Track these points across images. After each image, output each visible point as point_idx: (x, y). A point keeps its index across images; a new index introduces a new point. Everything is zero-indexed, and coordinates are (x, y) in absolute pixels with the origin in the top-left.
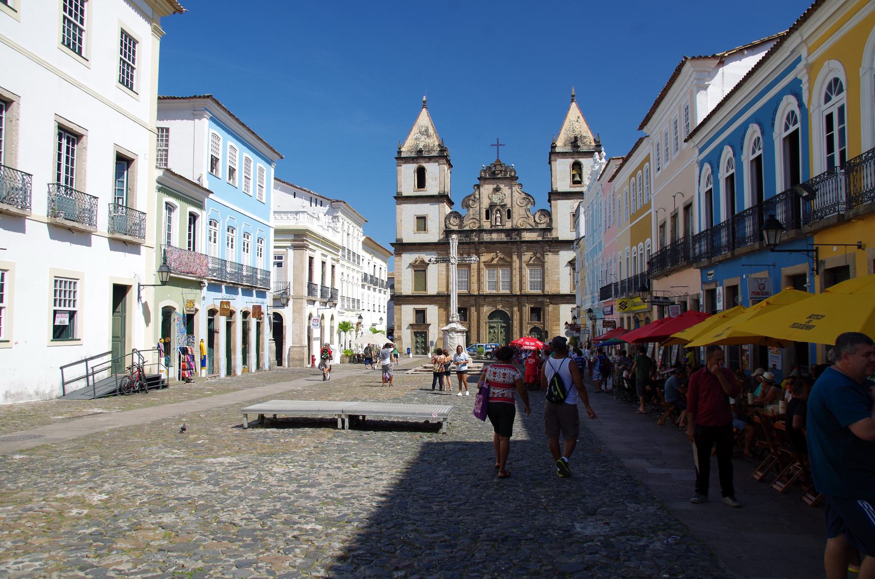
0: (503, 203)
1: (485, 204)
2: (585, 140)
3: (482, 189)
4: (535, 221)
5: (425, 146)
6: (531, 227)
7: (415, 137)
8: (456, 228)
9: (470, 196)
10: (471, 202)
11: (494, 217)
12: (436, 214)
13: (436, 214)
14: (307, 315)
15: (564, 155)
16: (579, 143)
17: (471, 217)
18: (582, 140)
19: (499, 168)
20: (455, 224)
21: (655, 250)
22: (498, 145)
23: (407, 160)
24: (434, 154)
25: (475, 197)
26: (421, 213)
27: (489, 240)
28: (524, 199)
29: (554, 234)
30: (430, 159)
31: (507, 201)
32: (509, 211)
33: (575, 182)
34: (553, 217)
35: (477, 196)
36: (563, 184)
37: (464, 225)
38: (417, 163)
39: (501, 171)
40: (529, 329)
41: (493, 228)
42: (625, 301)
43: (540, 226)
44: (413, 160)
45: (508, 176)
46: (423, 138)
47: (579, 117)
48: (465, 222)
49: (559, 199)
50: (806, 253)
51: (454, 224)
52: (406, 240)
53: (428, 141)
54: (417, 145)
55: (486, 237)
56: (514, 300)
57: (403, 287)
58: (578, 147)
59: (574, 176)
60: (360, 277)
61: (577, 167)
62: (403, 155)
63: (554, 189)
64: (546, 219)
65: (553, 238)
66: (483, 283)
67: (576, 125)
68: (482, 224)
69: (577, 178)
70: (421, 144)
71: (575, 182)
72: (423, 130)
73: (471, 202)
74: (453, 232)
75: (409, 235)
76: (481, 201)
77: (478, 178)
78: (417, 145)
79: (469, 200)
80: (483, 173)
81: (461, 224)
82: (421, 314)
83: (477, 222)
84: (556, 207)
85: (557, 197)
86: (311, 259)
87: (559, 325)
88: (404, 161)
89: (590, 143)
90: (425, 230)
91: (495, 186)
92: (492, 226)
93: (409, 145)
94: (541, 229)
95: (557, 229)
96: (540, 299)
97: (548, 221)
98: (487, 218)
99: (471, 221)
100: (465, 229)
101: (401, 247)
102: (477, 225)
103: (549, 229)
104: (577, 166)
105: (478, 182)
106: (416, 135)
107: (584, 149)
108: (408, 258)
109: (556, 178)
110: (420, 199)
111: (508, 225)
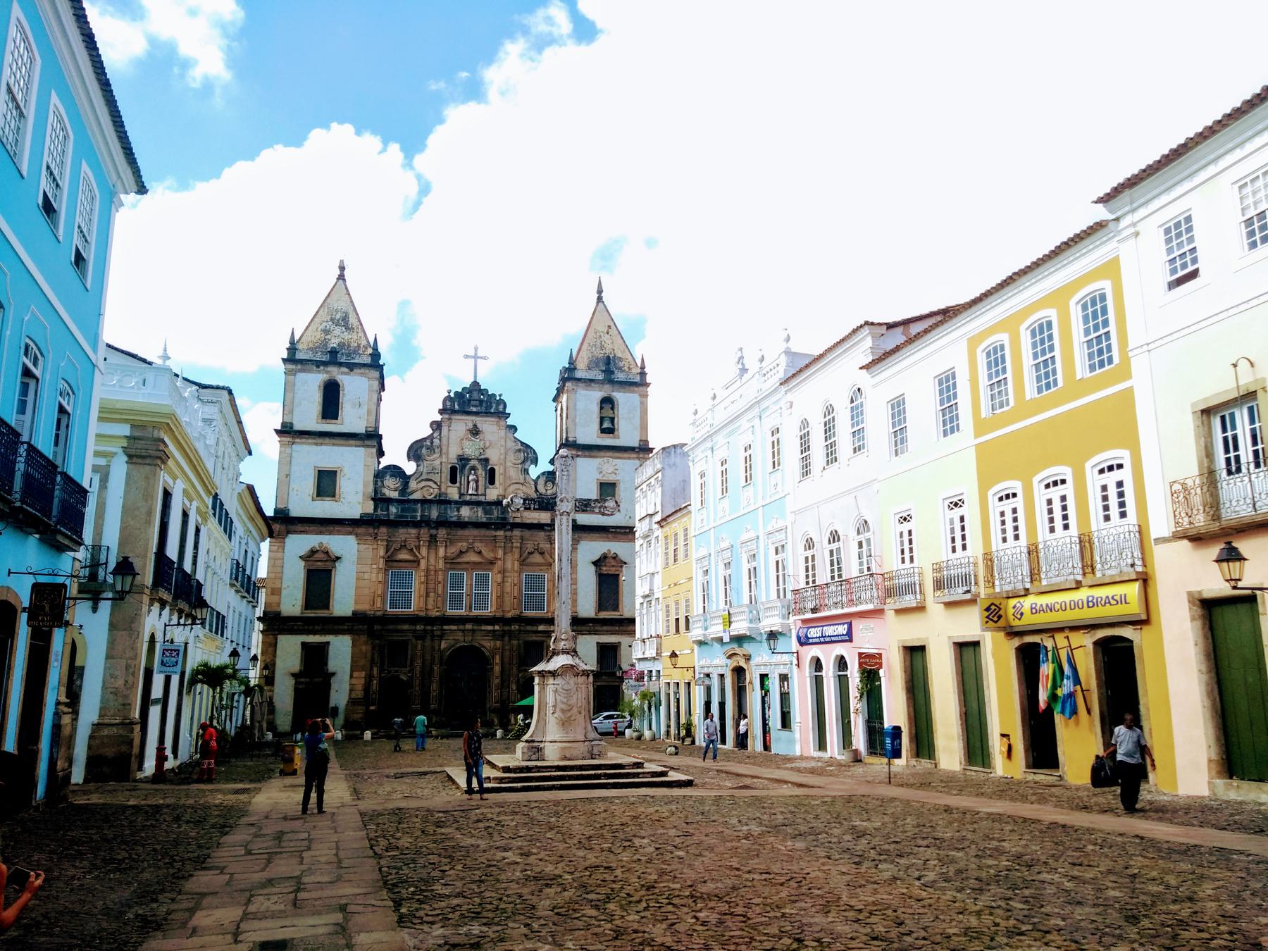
2: (621, 364)
3: (445, 430)
4: (536, 490)
5: (342, 345)
7: (323, 327)
8: (395, 495)
9: (425, 439)
10: (424, 451)
11: (464, 482)
16: (612, 367)
17: (424, 477)
18: (615, 364)
19: (475, 395)
20: (392, 486)
22: (476, 357)
25: (432, 443)
26: (327, 465)
27: (454, 519)
28: (519, 450)
30: (351, 367)
31: (494, 456)
32: (492, 471)
33: (603, 431)
35: (436, 442)
36: (589, 433)
37: (409, 490)
38: (327, 372)
39: (481, 402)
41: (468, 498)
44: (318, 367)
45: (492, 411)
46: (338, 331)
47: (609, 327)
48: (413, 485)
49: (578, 456)
51: (391, 489)
52: (295, 512)
53: (346, 336)
54: (326, 342)
55: (453, 515)
56: (497, 627)
57: (283, 600)
59: (602, 420)
62: (300, 356)
63: (571, 439)
66: (420, 596)
67: (606, 338)
69: (606, 425)
70: (333, 341)
71: (603, 431)
73: (424, 451)
74: (389, 501)
75: (305, 504)
78: (326, 342)
80: (448, 403)
81: (404, 489)
82: (315, 658)
83: (434, 486)
86: (167, 495)
88: (299, 367)
90: (334, 496)
91: (470, 426)
92: (461, 495)
93: (310, 339)
98: (453, 480)
99: (423, 484)
100: (411, 497)
102: (436, 491)
104: (607, 402)
105: (438, 418)
106: (325, 324)
107: (620, 376)
108: (299, 544)
109: (574, 420)
110: (327, 440)
111: (493, 494)
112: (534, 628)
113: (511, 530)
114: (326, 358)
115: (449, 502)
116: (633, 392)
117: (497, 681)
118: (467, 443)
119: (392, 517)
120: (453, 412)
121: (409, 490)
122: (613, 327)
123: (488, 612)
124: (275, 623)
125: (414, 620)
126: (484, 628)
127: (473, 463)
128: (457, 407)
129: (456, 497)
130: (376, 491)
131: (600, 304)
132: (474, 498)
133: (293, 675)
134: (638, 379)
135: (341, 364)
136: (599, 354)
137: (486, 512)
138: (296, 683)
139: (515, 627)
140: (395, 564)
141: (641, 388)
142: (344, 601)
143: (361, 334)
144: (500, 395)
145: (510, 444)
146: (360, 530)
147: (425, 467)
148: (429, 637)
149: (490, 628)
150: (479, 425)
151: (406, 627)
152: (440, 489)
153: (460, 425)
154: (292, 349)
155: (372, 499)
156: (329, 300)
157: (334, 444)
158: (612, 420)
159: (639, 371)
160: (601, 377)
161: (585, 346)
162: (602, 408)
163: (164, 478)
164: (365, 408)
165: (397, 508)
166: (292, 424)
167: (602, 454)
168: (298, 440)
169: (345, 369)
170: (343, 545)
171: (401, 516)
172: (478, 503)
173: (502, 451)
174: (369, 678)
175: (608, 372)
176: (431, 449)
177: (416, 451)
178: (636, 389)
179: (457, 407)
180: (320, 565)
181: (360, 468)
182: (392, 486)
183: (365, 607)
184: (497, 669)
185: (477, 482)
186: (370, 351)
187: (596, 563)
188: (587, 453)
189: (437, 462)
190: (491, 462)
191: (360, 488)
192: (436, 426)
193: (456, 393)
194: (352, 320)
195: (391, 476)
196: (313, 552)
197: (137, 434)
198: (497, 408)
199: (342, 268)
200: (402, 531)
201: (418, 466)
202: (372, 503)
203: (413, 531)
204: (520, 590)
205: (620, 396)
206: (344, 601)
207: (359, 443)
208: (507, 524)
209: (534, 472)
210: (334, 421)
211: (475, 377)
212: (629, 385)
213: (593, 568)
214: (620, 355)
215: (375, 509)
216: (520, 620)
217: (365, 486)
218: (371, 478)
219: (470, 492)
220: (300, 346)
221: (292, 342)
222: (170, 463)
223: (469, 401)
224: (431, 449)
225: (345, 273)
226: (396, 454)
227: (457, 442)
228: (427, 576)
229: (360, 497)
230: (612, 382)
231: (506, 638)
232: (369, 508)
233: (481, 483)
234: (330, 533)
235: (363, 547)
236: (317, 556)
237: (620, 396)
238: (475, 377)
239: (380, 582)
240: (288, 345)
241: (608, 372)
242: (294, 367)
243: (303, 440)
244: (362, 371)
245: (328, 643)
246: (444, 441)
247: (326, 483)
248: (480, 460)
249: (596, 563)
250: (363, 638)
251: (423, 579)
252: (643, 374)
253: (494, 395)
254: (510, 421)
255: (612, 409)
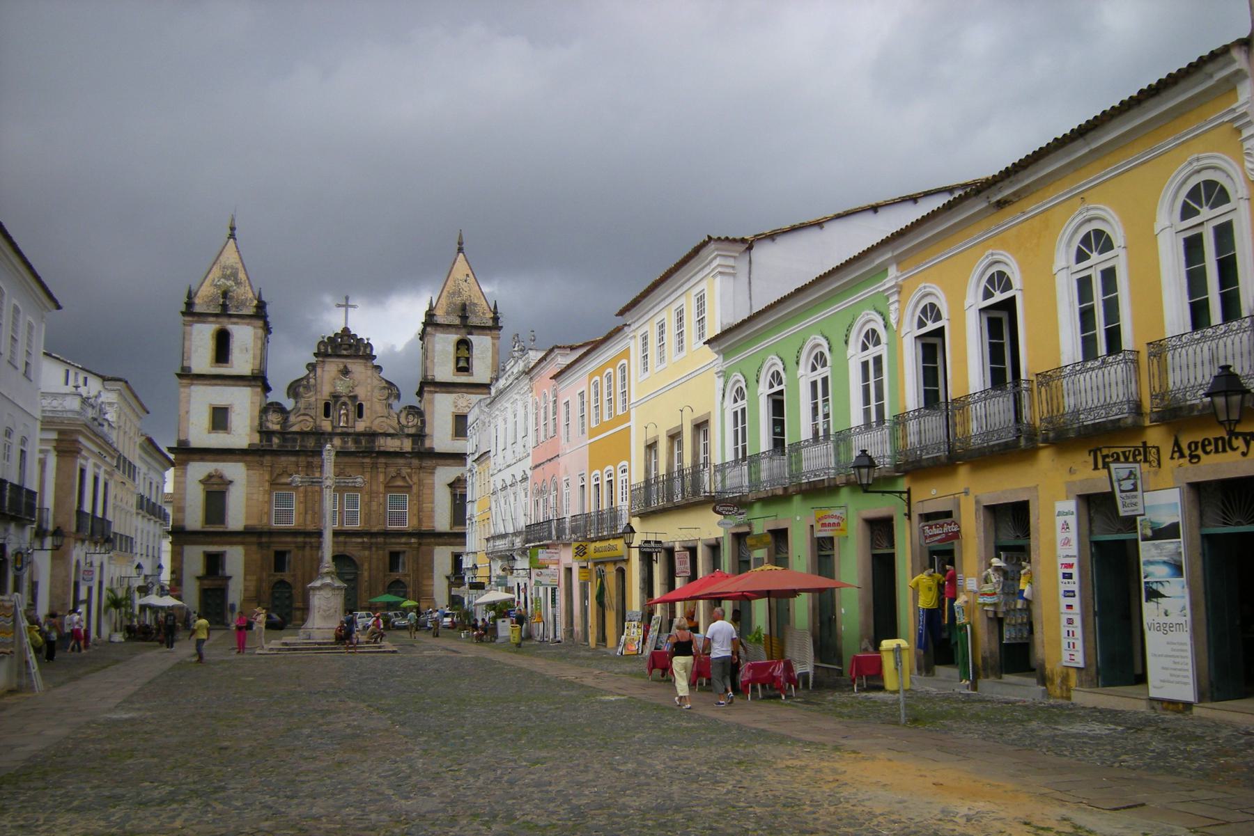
0: (351, 394)
1: (326, 391)
3: (319, 370)
6: (392, 431)
8: (277, 427)
9: (302, 379)
10: (301, 389)
12: (242, 403)
13: (242, 403)
14: (74, 563)
15: (447, 327)
17: (302, 412)
20: (275, 420)
21: (638, 477)
23: (202, 317)
24: (245, 312)
25: (308, 382)
28: (384, 388)
29: (427, 444)
31: (361, 392)
32: (360, 407)
33: (460, 370)
34: (427, 418)
35: (312, 381)
36: (444, 371)
38: (219, 323)
39: (350, 346)
40: (387, 584)
41: (339, 430)
42: (584, 544)
43: (406, 431)
48: (292, 419)
49: (436, 392)
50: (898, 495)
51: (274, 423)
56: (365, 540)
58: (467, 317)
59: (458, 360)
60: (134, 500)
61: (463, 348)
63: (430, 377)
64: (416, 420)
65: (426, 449)
68: (318, 423)
69: (462, 364)
71: (460, 370)
72: (228, 272)
73: (301, 389)
74: (273, 433)
75: (200, 434)
76: (319, 389)
77: (315, 354)
79: (299, 386)
80: (322, 348)
81: (285, 421)
82: (214, 563)
83: (311, 420)
84: (432, 402)
85: (432, 389)
86: (83, 471)
87: (431, 578)
88: (196, 319)
89: (484, 313)
91: (341, 366)
92: (334, 427)
93: (204, 294)
94: (408, 436)
95: (432, 436)
96: (403, 540)
97: (419, 424)
98: (327, 414)
99: (301, 418)
101: (186, 453)
103: (419, 436)
104: (464, 344)
105: (314, 360)
107: (474, 320)
108: (199, 470)
109: (433, 361)
110: (219, 382)
111: (361, 426)
112: (398, 541)
113: (377, 457)
114: (218, 311)
115: (323, 434)
116: (487, 335)
117: (366, 584)
118: (338, 382)
119: (275, 447)
120: (326, 355)
121: (290, 423)
122: (471, 275)
123: (358, 526)
124: (180, 536)
125: (294, 533)
126: (354, 540)
127: (343, 399)
128: (330, 350)
129: (329, 429)
130: (261, 425)
131: (461, 254)
132: (345, 430)
133: (198, 578)
134: (490, 323)
135: (231, 316)
136: (458, 300)
137: (357, 442)
138: (201, 584)
139: (380, 540)
140: (278, 487)
141: (493, 332)
142: (237, 516)
143: (248, 288)
144: (368, 339)
145: (376, 382)
146: (249, 458)
147: (302, 405)
148: (308, 548)
149: (360, 540)
150: (350, 367)
151: (289, 539)
152: (315, 422)
153: (331, 368)
154: (190, 304)
155: (259, 432)
156: (221, 258)
157: (225, 385)
158: (467, 360)
159: (492, 315)
160: (457, 321)
161: (445, 294)
162: (458, 349)
163: (80, 461)
164: (252, 352)
165: (278, 438)
166: (190, 368)
167: (458, 390)
168: (195, 382)
169: (235, 320)
170: (235, 471)
171: (283, 446)
172: (348, 434)
173: (369, 389)
174: (260, 580)
175: (464, 318)
176: (307, 388)
177: (295, 389)
178: (488, 332)
179: (330, 350)
180: (216, 488)
181: (247, 404)
182: (275, 420)
183: (253, 522)
184: (366, 574)
185: (347, 415)
186: (255, 302)
187: (451, 485)
188: (444, 389)
189: (313, 399)
190: (359, 398)
191: (248, 422)
192: (312, 367)
193: (329, 338)
194: (242, 276)
195: (274, 411)
196: (210, 476)
197: (62, 437)
198: (365, 351)
199: (233, 229)
200: (283, 459)
201: (296, 403)
202: (258, 434)
203: (293, 459)
204: (385, 508)
205: (474, 339)
206: (237, 516)
207: (246, 383)
208: (373, 452)
209: (397, 406)
210: (225, 365)
211: (346, 323)
212: (482, 329)
213: (448, 490)
214: (476, 302)
215: (261, 441)
216: (386, 534)
217: (252, 419)
218: (257, 413)
219: (342, 424)
220: (197, 301)
221: (190, 296)
222: (84, 453)
223: (341, 345)
224: (307, 388)
225: (236, 232)
226: (278, 395)
227: (329, 379)
228: (305, 496)
229: (248, 429)
230: (465, 326)
231: (374, 549)
232: (256, 439)
233: (351, 416)
234: (224, 461)
235: (251, 472)
236: (213, 480)
237: (474, 339)
238: (346, 323)
239: (266, 502)
240: (186, 300)
241: (464, 318)
242: (190, 319)
243: (199, 382)
244: (247, 321)
245: (225, 552)
246: (319, 380)
247: (220, 418)
248: (350, 397)
249: (451, 485)
250: (254, 548)
251: (302, 499)
252: (496, 319)
253: (362, 339)
254: (376, 362)
255: (468, 349)
